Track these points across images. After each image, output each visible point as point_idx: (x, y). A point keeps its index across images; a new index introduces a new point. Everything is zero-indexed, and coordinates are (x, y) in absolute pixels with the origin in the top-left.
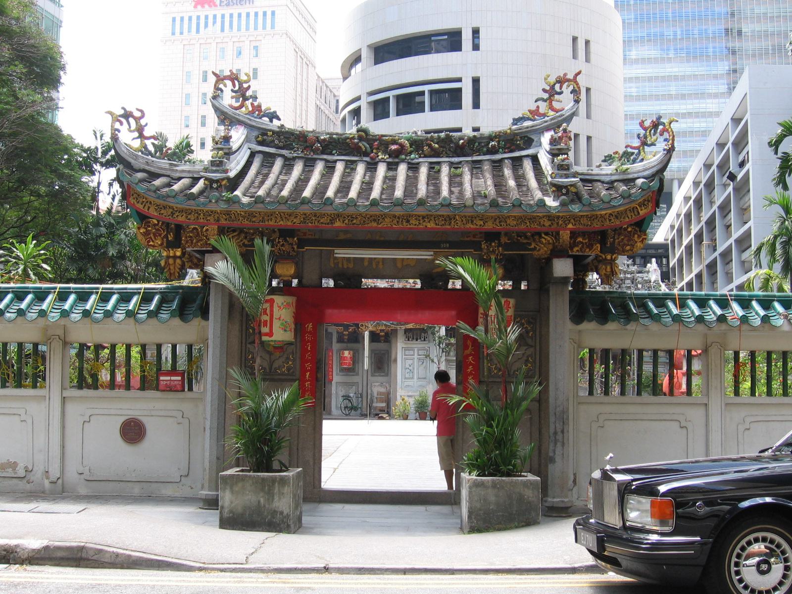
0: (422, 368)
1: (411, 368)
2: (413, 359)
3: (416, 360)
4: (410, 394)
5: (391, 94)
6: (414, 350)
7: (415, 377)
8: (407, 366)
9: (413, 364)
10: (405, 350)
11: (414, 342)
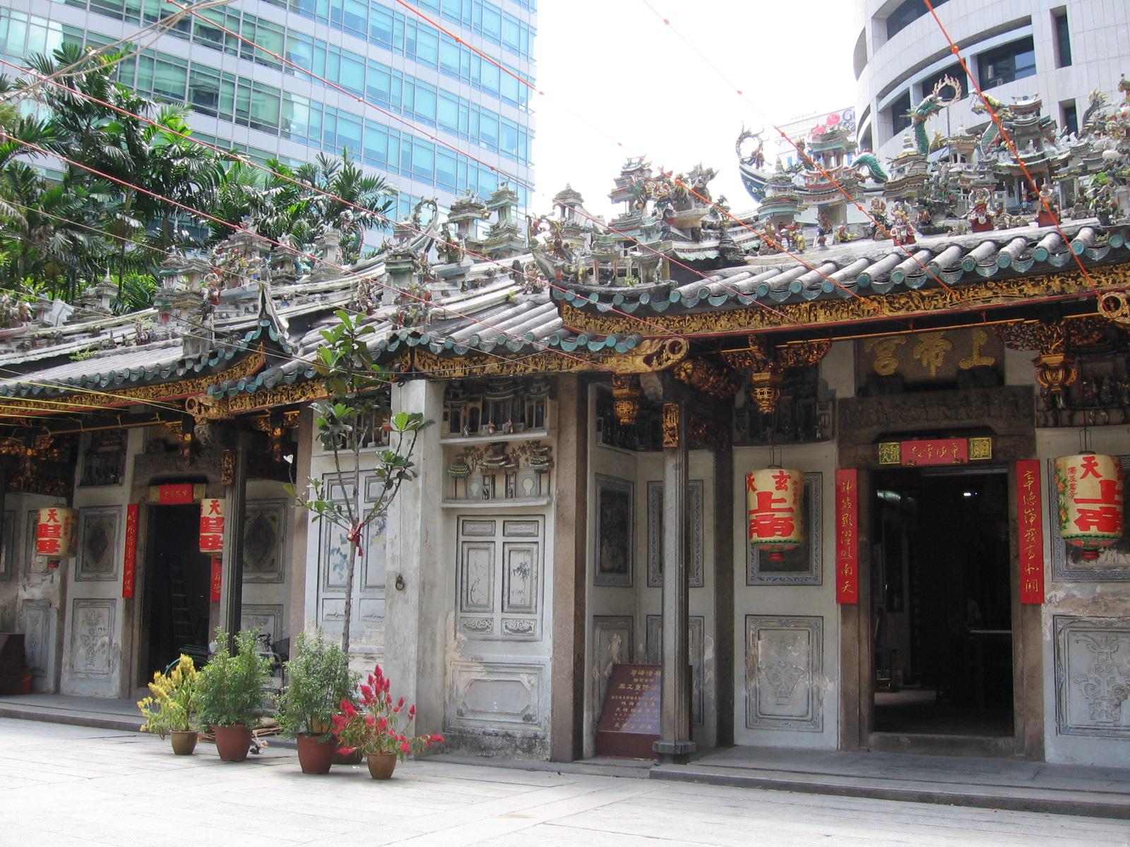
5: (909, 84)
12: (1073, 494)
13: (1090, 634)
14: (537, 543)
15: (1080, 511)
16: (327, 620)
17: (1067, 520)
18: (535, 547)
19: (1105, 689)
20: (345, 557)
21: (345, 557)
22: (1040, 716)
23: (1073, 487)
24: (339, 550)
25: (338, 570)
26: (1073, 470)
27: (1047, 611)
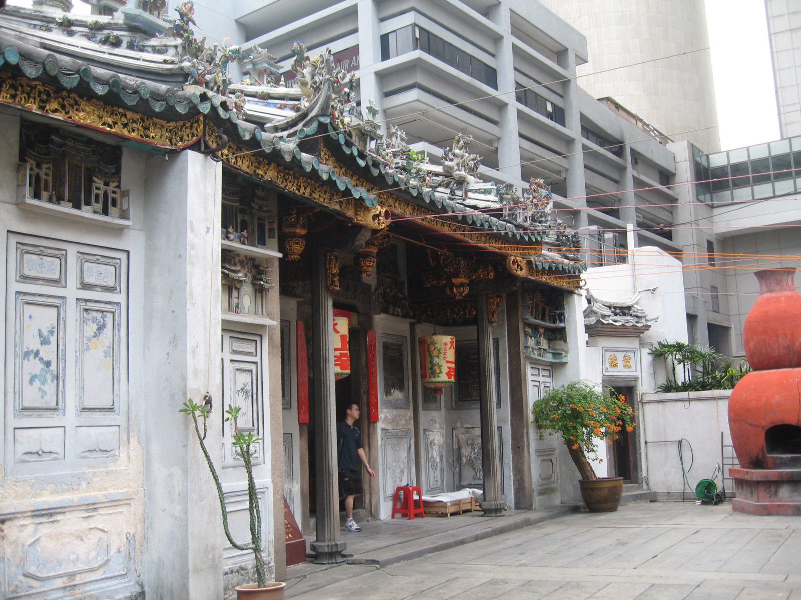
0: (96, 355)
1: (48, 353)
2: (57, 305)
3: (72, 312)
4: (47, 499)
6: (62, 258)
7: (71, 402)
8: (33, 343)
9: (59, 327)
10: (24, 249)
11: (66, 208)
12: (445, 358)
13: (392, 440)
14: (255, 363)
15: (449, 368)
16: (23, 461)
17: (441, 372)
18: (253, 367)
19: (398, 471)
20: (48, 364)
21: (48, 364)
22: (379, 491)
23: (445, 354)
24: (37, 354)
25: (37, 383)
26: (446, 344)
27: (380, 425)
